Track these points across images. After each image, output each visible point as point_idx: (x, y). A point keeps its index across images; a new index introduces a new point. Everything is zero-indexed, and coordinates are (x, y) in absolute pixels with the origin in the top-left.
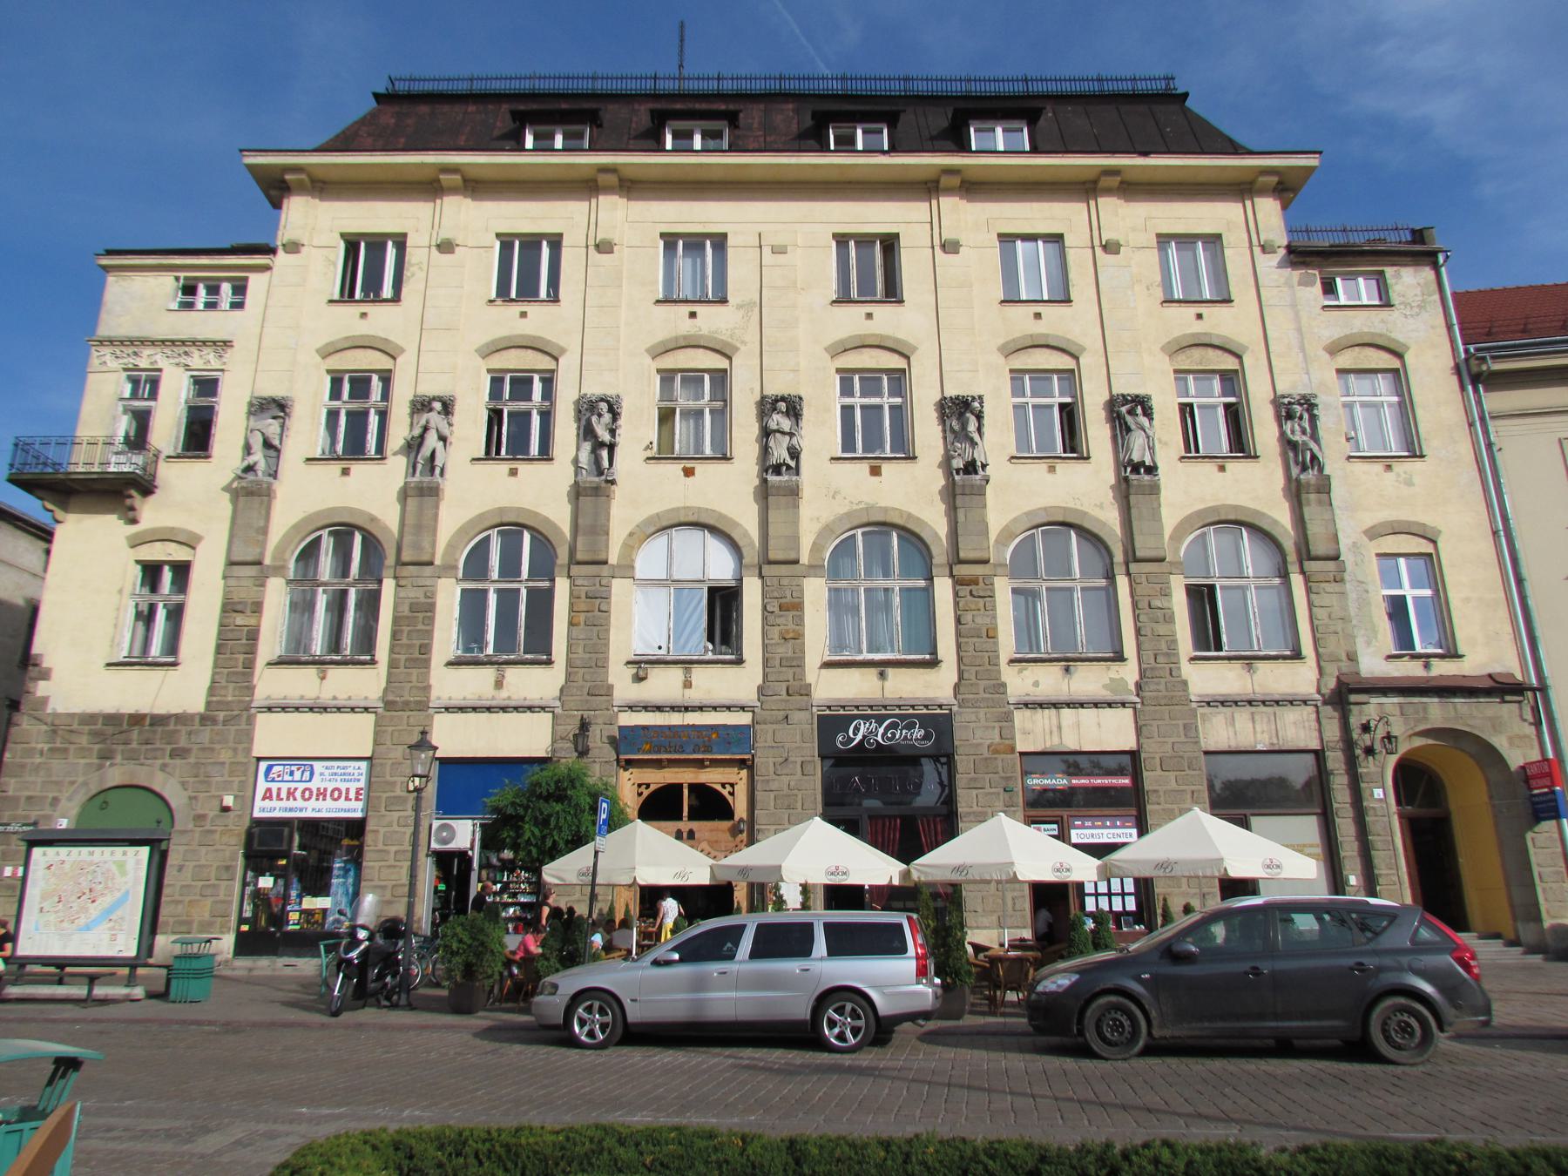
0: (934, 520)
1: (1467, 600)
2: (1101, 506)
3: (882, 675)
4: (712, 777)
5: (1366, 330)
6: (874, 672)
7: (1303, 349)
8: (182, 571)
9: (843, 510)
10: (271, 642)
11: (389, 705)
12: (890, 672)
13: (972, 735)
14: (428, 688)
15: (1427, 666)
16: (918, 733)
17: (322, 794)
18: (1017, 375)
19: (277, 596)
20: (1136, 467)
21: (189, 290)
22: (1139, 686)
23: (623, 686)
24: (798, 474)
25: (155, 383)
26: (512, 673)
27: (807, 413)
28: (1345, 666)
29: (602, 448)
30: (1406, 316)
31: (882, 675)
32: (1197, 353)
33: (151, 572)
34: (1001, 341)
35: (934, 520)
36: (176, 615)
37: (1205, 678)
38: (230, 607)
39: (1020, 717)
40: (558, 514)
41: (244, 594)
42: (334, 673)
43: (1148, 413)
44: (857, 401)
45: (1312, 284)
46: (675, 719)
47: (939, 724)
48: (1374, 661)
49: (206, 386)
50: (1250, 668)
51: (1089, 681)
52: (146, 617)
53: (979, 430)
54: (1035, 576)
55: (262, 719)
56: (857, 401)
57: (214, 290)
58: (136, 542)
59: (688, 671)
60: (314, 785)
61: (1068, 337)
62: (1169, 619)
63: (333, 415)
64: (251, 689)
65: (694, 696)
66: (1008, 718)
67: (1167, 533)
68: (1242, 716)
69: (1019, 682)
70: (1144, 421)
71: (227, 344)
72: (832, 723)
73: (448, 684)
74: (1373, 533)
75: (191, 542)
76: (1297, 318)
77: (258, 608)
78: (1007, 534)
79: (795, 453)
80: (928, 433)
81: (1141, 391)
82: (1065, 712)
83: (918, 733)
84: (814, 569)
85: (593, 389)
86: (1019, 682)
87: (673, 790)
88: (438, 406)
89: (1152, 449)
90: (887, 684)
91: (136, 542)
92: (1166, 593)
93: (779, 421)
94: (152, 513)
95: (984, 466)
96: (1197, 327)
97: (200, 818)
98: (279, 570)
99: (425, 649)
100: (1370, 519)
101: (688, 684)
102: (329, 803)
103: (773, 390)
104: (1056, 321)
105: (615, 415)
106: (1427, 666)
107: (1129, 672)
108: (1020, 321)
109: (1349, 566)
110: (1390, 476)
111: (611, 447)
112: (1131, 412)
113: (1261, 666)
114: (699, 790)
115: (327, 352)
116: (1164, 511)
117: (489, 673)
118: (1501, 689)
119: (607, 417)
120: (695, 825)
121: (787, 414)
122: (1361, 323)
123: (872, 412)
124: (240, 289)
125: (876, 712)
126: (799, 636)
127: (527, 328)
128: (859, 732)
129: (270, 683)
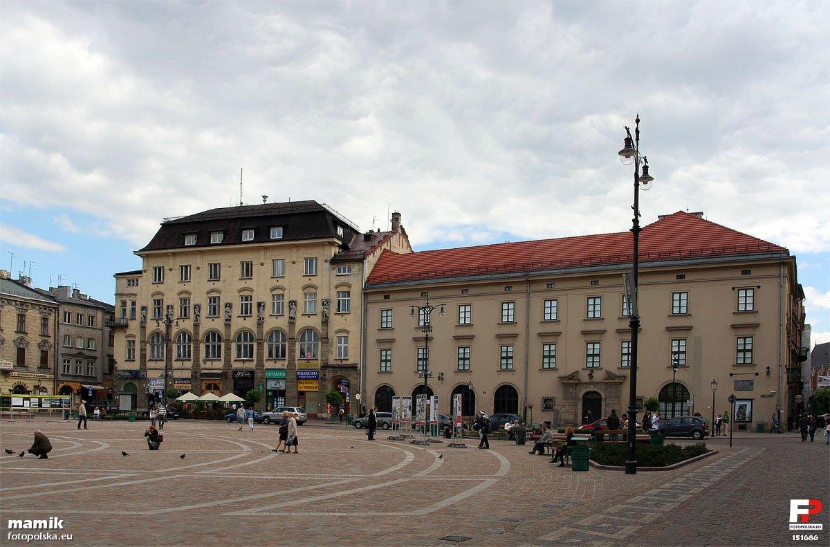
0: (255, 330)
4: (216, 382)
8: (134, 342)
10: (148, 358)
13: (258, 375)
18: (273, 296)
19: (148, 347)
20: (292, 318)
21: (129, 281)
23: (202, 365)
24: (230, 320)
25: (126, 302)
28: (325, 362)
33: (129, 342)
35: (255, 330)
36: (134, 350)
38: (141, 350)
40: (191, 329)
41: (143, 347)
42: (158, 363)
43: (295, 305)
44: (244, 302)
46: (210, 371)
47: (252, 372)
48: (331, 361)
49: (134, 303)
51: (279, 365)
52: (129, 350)
53: (264, 309)
56: (244, 302)
57: (133, 281)
60: (157, 383)
63: (155, 308)
65: (213, 367)
67: (296, 332)
69: (268, 365)
70: (294, 307)
71: (136, 295)
72: (235, 372)
73: (176, 365)
75: (134, 337)
76: (330, 280)
77: (145, 350)
79: (230, 317)
80: (255, 310)
81: (294, 299)
84: (233, 341)
85: (196, 303)
86: (268, 365)
87: (211, 384)
89: (295, 313)
91: (127, 337)
94: (129, 332)
96: (309, 282)
98: (148, 342)
99: (171, 358)
103: (227, 302)
104: (281, 282)
105: (200, 309)
107: (286, 363)
108: (274, 283)
111: (199, 315)
112: (292, 304)
114: (215, 384)
115: (153, 295)
116: (296, 327)
117: (181, 362)
118: (354, 367)
122: (344, 280)
123: (246, 305)
124: (137, 281)
125: (242, 370)
126: (230, 355)
127: (185, 288)
129: (149, 365)
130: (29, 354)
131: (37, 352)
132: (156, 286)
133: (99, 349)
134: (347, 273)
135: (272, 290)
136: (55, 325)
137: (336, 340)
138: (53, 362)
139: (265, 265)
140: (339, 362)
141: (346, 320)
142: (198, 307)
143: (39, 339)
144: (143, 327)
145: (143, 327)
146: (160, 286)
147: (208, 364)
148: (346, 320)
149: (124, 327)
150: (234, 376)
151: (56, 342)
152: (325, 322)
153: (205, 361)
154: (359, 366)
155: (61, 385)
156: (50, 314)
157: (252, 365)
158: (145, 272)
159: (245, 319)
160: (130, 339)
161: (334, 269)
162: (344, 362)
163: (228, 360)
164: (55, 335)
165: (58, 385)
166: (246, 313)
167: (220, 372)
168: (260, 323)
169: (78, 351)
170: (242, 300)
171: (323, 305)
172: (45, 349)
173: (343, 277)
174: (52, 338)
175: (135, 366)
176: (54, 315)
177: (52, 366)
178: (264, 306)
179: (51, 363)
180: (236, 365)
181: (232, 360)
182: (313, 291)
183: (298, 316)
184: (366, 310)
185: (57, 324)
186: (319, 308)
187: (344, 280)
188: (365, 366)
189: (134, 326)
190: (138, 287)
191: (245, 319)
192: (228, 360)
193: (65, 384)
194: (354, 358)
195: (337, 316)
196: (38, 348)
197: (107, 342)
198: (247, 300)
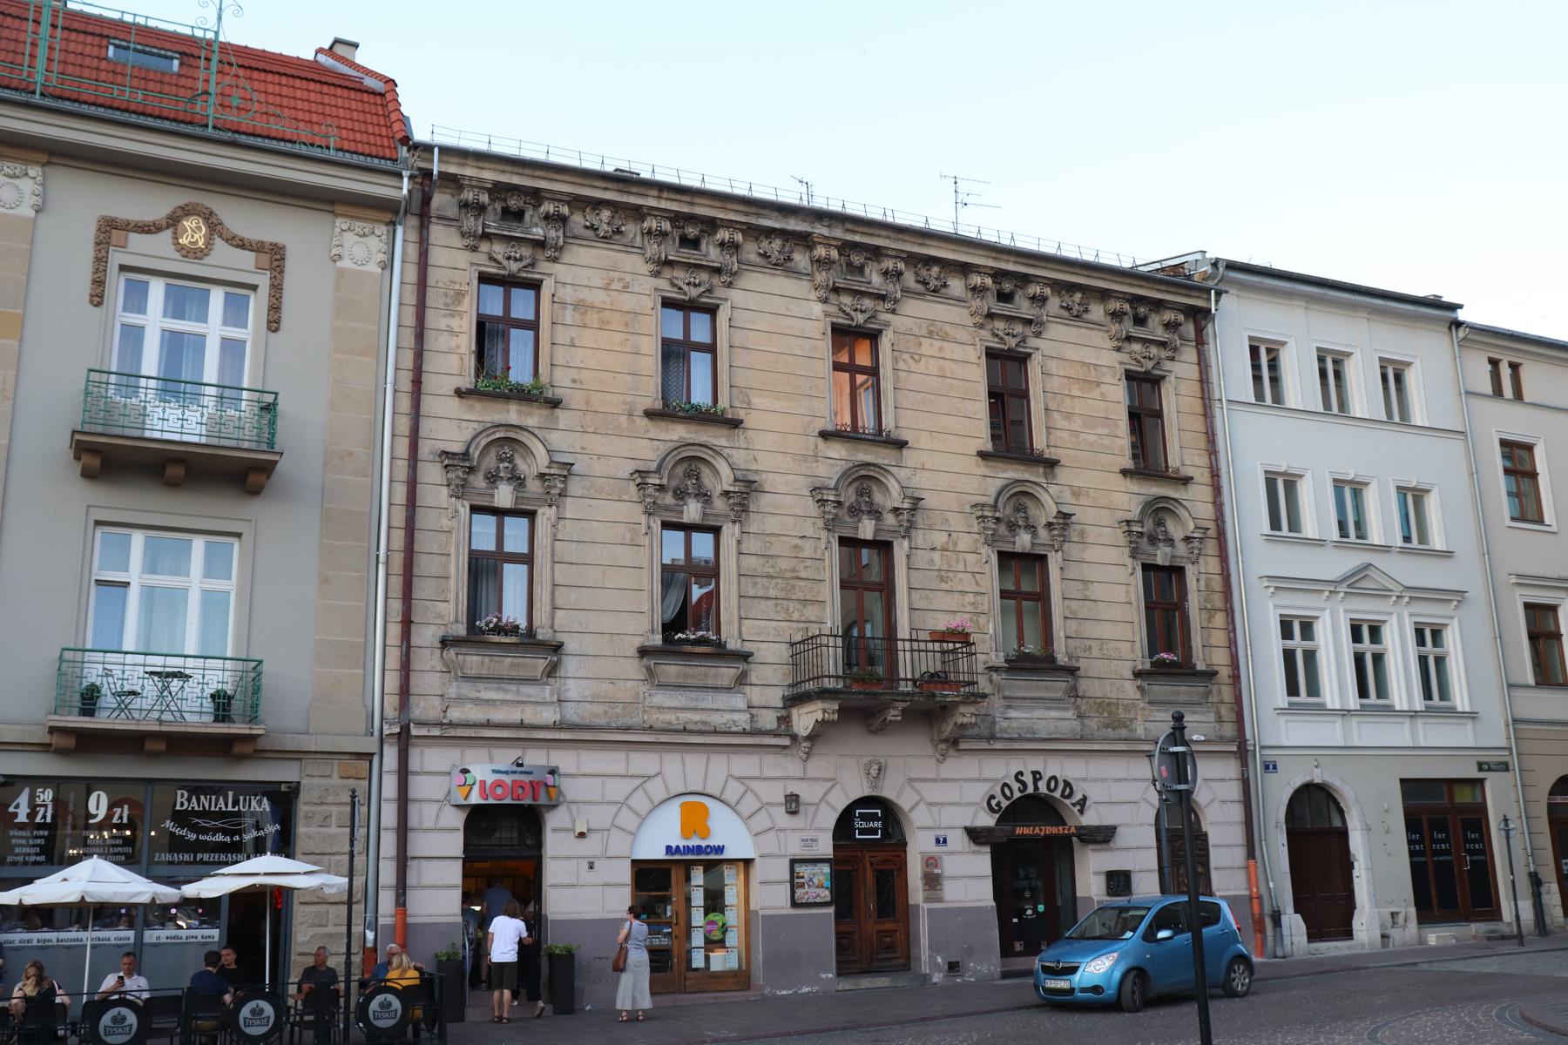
130: (1074, 589)
131: (1121, 574)
133: (1467, 549)
143: (1129, 497)
169: (1352, 560)
172: (1161, 556)
196: (1122, 555)
197: (1502, 505)
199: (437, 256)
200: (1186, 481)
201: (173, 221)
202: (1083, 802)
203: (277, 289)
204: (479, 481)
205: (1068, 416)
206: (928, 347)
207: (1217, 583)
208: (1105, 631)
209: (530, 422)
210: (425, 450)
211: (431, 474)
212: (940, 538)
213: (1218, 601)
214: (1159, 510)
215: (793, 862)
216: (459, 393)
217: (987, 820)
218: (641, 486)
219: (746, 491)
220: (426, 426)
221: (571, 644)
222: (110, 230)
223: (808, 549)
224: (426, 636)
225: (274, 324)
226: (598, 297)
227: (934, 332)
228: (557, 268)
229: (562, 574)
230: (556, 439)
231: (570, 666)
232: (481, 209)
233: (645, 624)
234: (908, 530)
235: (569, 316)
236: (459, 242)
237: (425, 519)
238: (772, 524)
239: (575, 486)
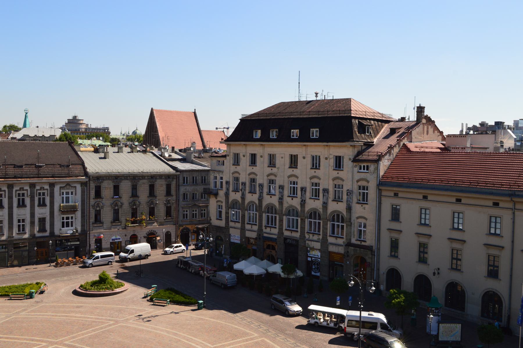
1: (369, 232)
2: (320, 208)
3: (292, 233)
5: (363, 177)
6: (290, 232)
7: (352, 181)
9: (288, 205)
11: (241, 229)
12: (293, 232)
14: (245, 227)
15: (361, 243)
16: (295, 242)
17: (236, 239)
22: (322, 239)
23: (264, 230)
25: (216, 177)
26: (253, 226)
27: (285, 188)
29: (261, 193)
30: (370, 175)
31: (292, 233)
32: (337, 180)
34: (309, 177)
37: (331, 240)
39: (307, 242)
42: (236, 223)
43: (328, 193)
44: (292, 186)
45: (356, 167)
47: (297, 241)
48: (353, 241)
49: (222, 178)
50: (336, 239)
51: (316, 237)
54: (312, 219)
55: (231, 229)
56: (292, 186)
58: (217, 202)
59: (270, 229)
61: (319, 176)
62: (327, 229)
64: (229, 225)
66: (305, 242)
68: (334, 247)
70: (326, 194)
72: (286, 239)
73: (248, 227)
74: (358, 218)
77: (229, 213)
78: (308, 212)
79: (282, 196)
82: (312, 242)
83: (295, 242)
85: (260, 182)
88: (243, 184)
89: (327, 199)
90: (292, 234)
92: (327, 224)
93: (281, 190)
94: (219, 199)
95: (305, 201)
96: (337, 175)
97: (225, 241)
99: (245, 221)
100: (357, 216)
101: (270, 230)
102: (237, 241)
106: (361, 243)
107: (321, 237)
109: (353, 223)
110: (362, 207)
112: (325, 192)
113: (338, 239)
114: (273, 246)
119: (261, 188)
120: (272, 250)
121: (282, 188)
122: (362, 176)
127: (253, 171)
128: (288, 241)
132: (235, 166)
134: (366, 171)
135: (311, 178)
136: (176, 187)
137: (357, 225)
138: (175, 213)
139: (306, 159)
140: (359, 243)
141: (365, 209)
142: (261, 186)
144: (227, 195)
145: (227, 195)
146: (238, 167)
147: (268, 230)
148: (365, 209)
149: (216, 195)
150: (284, 242)
151: (178, 200)
152: (349, 209)
153: (266, 227)
154: (374, 248)
155: (181, 228)
156: (173, 181)
157: (297, 235)
158: (228, 156)
159: (292, 199)
160: (219, 203)
161: (356, 166)
162: (363, 243)
163: (281, 229)
164: (176, 195)
165: (179, 229)
166: (294, 194)
167: (275, 237)
168: (303, 203)
170: (291, 184)
171: (347, 195)
173: (363, 174)
174: (174, 197)
175: (222, 223)
176: (175, 180)
177: (175, 216)
178: (305, 191)
179: (173, 213)
180: (287, 233)
181: (284, 229)
182: (340, 183)
183: (330, 200)
184: (380, 203)
185: (178, 186)
186: (345, 197)
187: (362, 176)
188: (379, 249)
189: (222, 193)
190: (223, 166)
191: (292, 199)
192: (281, 229)
193: (184, 226)
194: (370, 240)
195: (357, 205)
198: (294, 183)
199: (91, 185)
200: (173, 196)
201: (66, 186)
202: (157, 233)
203: (76, 191)
204: (95, 207)
205: (159, 191)
206: (143, 185)
207: (175, 207)
208: (161, 214)
209: (100, 200)
210: (90, 205)
211: (91, 207)
212: (143, 207)
213: (175, 209)
214: (168, 202)
215: (126, 241)
216: (93, 199)
217: (146, 235)
218: (111, 206)
219: (122, 204)
220: (91, 202)
221: (105, 222)
222: (61, 187)
223: (128, 210)
224: (91, 223)
225: (76, 195)
226: (107, 186)
227: (144, 184)
228: (103, 184)
229: (103, 215)
230: (103, 202)
231: (104, 224)
232: (95, 179)
233: (111, 219)
234: (139, 207)
235: (104, 189)
236: (92, 183)
237: (91, 212)
238: (124, 208)
239: (105, 206)
